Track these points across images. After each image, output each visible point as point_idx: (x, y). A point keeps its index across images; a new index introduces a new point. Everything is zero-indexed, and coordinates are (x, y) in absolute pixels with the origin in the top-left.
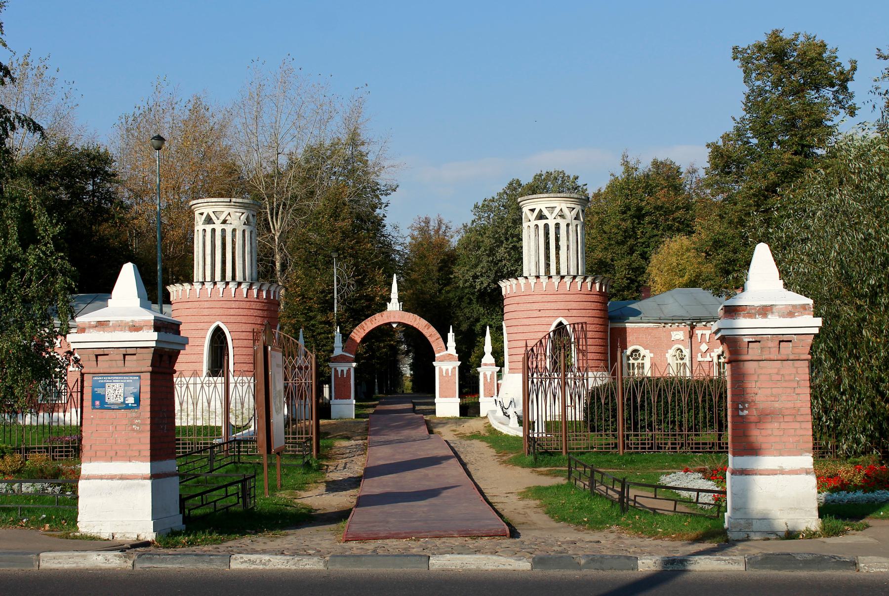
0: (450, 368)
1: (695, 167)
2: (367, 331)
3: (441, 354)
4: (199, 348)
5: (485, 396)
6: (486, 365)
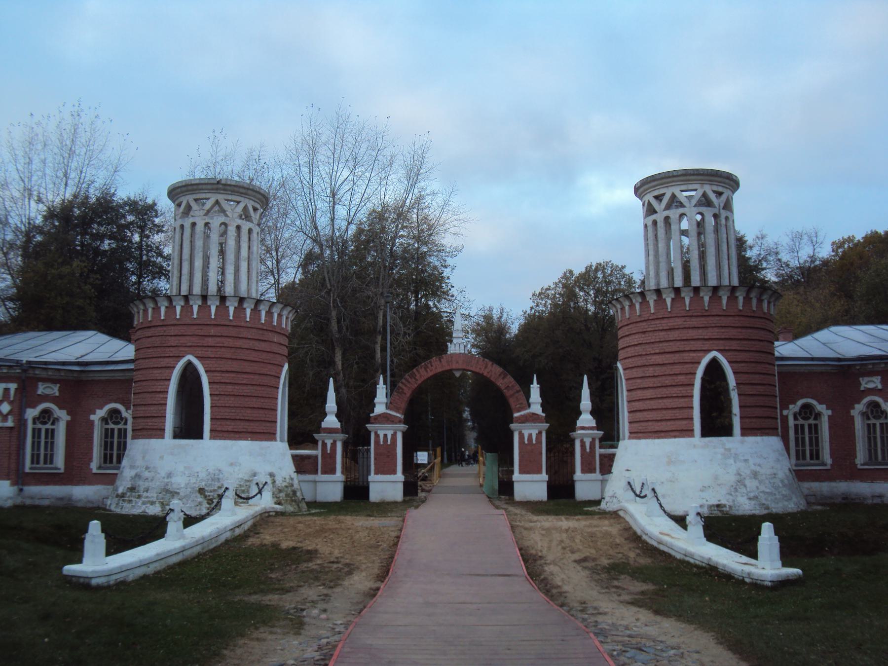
0: (534, 433)
1: (764, 232)
2: (419, 382)
4: (161, 396)
6: (583, 428)
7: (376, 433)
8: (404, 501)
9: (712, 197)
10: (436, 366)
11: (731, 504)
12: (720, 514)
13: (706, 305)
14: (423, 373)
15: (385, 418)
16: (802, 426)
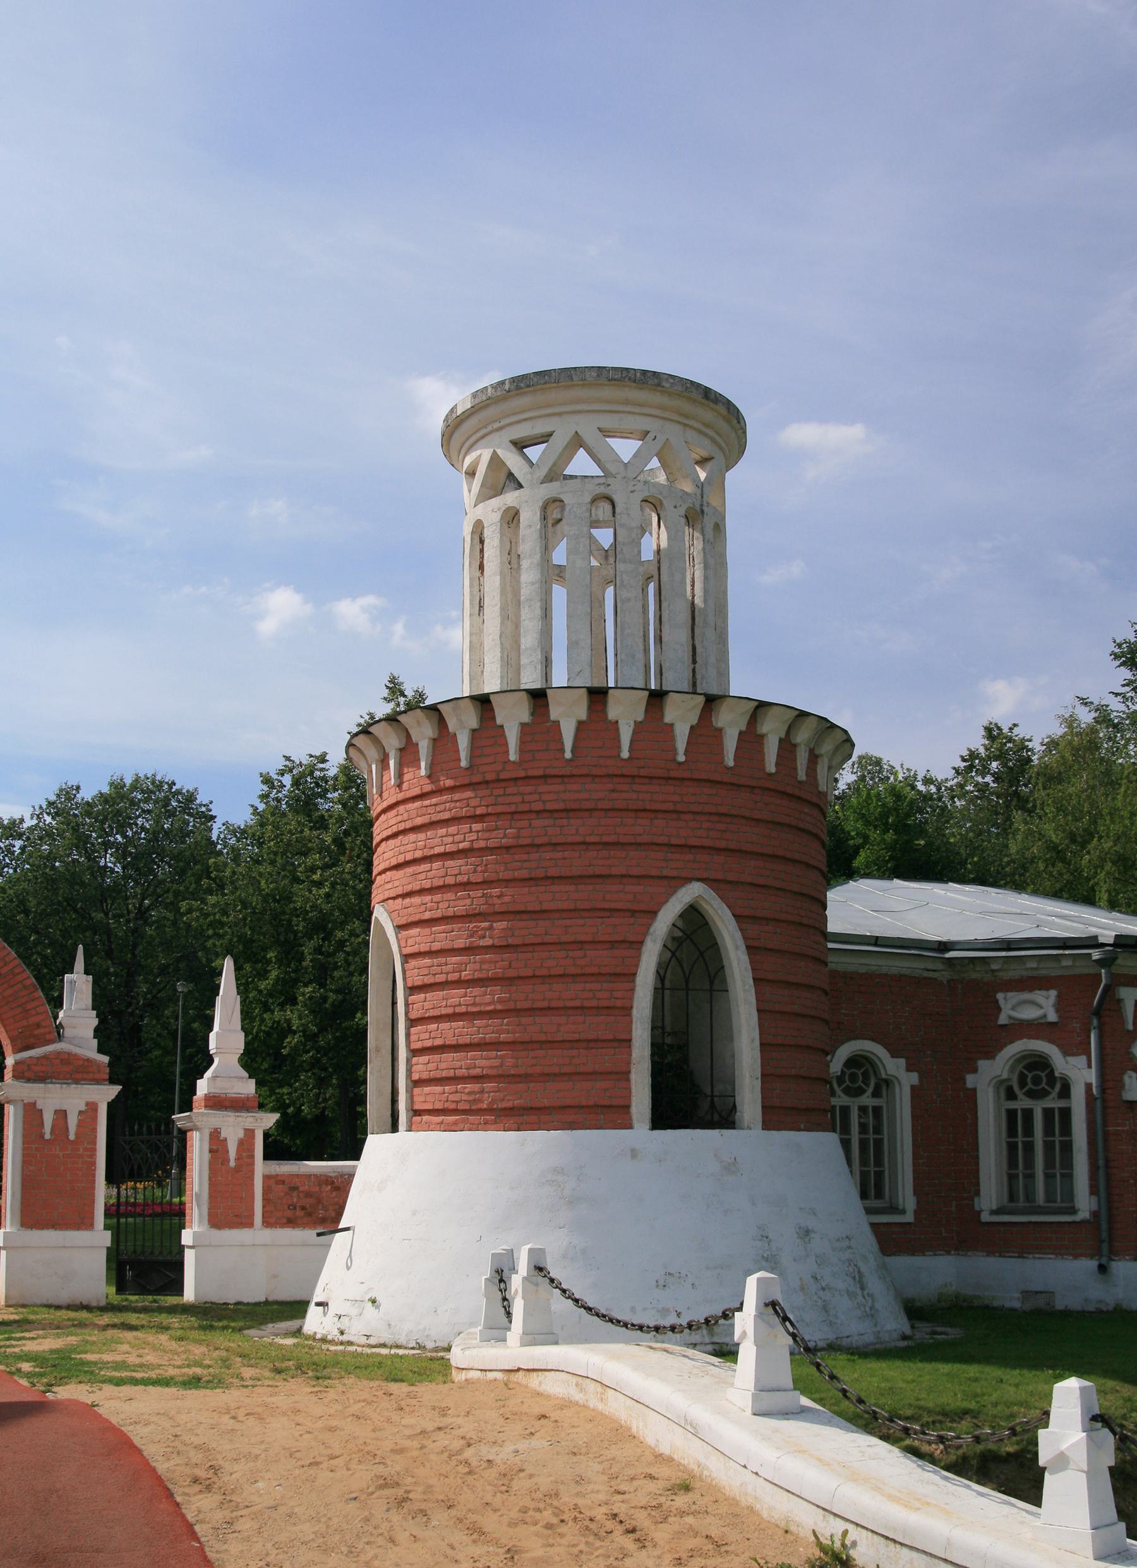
16: (1028, 1114)
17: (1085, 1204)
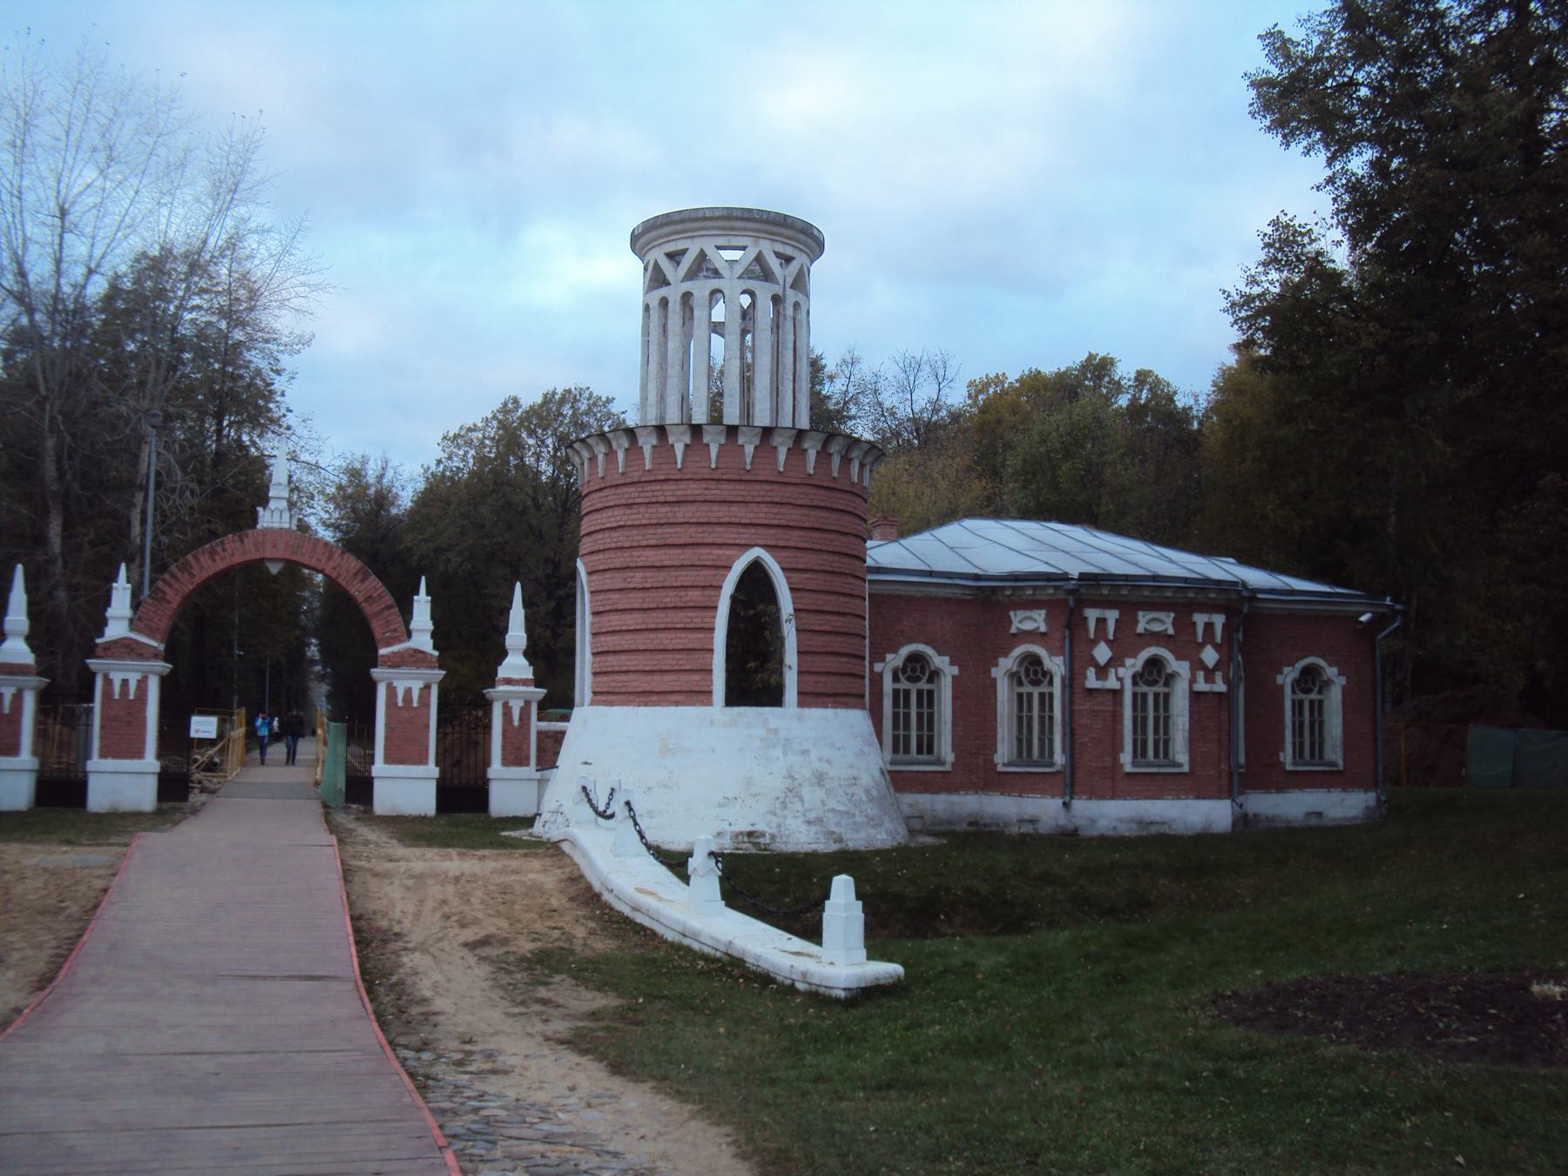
0: (417, 686)
2: (198, 580)
3: (395, 648)
5: (506, 762)
6: (508, 681)
7: (106, 677)
8: (159, 812)
9: (774, 263)
10: (233, 551)
11: (774, 831)
12: (754, 851)
13: (748, 460)
14: (206, 564)
15: (125, 649)
16: (907, 693)
17: (1059, 758)
